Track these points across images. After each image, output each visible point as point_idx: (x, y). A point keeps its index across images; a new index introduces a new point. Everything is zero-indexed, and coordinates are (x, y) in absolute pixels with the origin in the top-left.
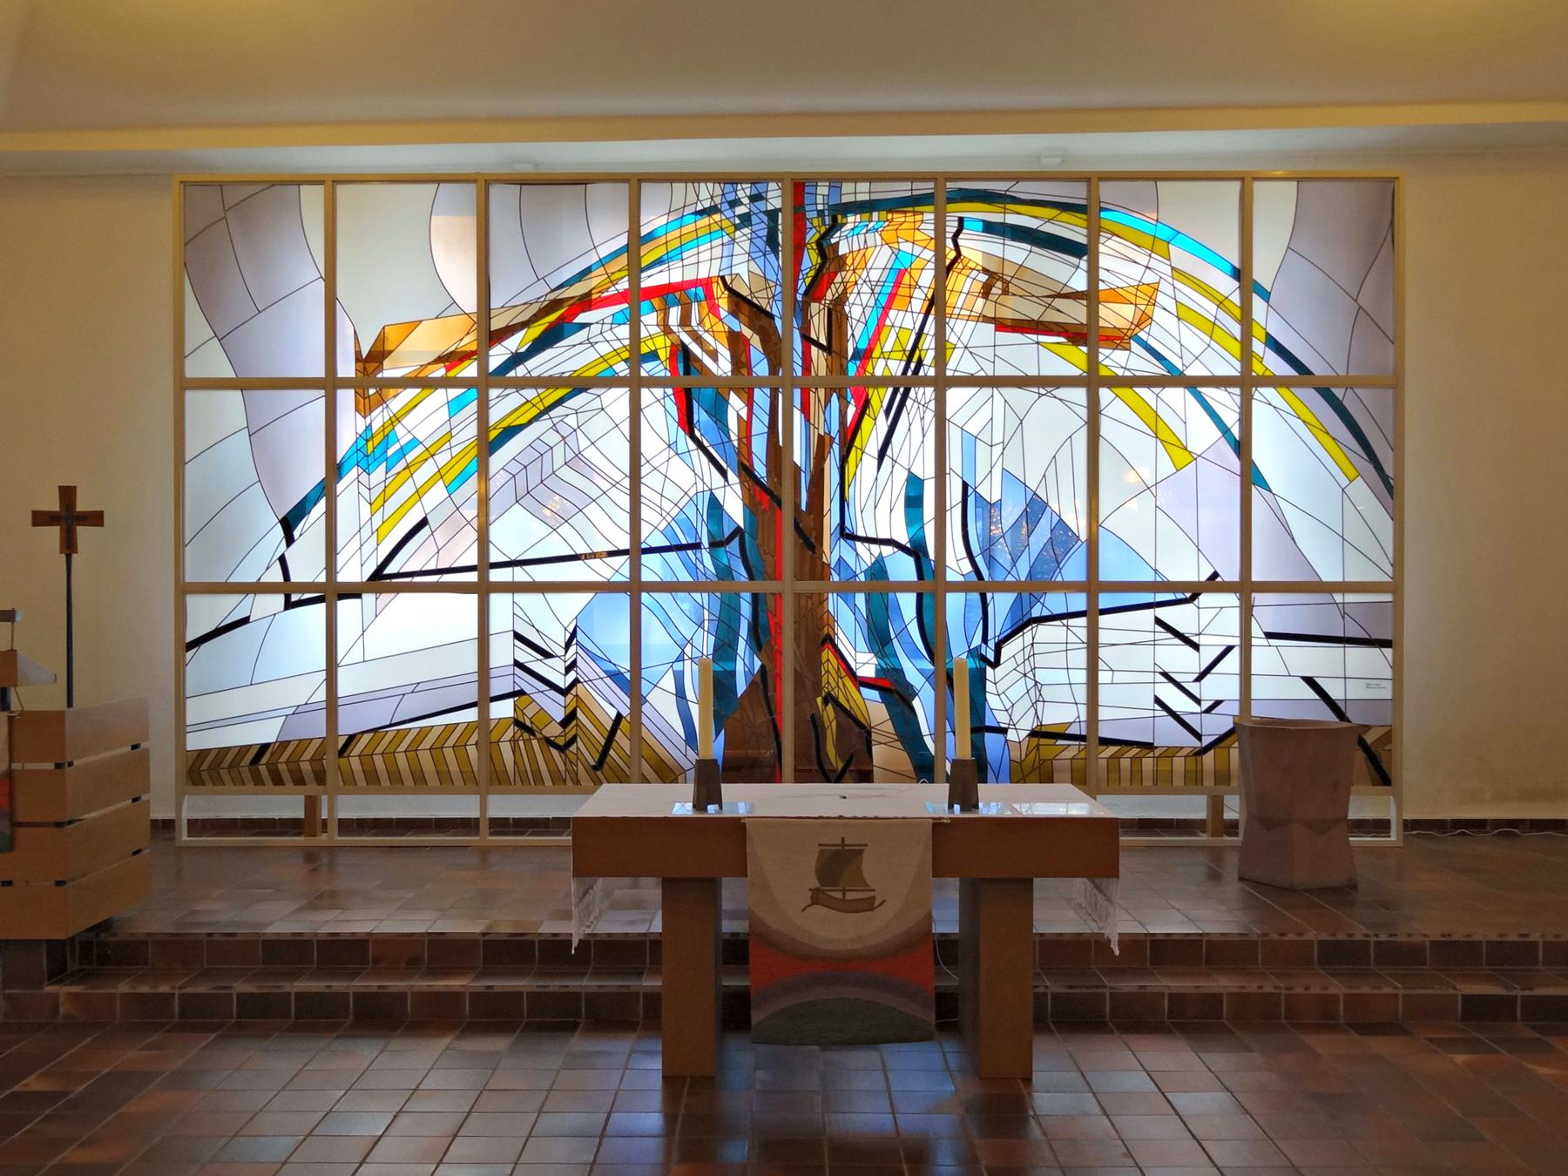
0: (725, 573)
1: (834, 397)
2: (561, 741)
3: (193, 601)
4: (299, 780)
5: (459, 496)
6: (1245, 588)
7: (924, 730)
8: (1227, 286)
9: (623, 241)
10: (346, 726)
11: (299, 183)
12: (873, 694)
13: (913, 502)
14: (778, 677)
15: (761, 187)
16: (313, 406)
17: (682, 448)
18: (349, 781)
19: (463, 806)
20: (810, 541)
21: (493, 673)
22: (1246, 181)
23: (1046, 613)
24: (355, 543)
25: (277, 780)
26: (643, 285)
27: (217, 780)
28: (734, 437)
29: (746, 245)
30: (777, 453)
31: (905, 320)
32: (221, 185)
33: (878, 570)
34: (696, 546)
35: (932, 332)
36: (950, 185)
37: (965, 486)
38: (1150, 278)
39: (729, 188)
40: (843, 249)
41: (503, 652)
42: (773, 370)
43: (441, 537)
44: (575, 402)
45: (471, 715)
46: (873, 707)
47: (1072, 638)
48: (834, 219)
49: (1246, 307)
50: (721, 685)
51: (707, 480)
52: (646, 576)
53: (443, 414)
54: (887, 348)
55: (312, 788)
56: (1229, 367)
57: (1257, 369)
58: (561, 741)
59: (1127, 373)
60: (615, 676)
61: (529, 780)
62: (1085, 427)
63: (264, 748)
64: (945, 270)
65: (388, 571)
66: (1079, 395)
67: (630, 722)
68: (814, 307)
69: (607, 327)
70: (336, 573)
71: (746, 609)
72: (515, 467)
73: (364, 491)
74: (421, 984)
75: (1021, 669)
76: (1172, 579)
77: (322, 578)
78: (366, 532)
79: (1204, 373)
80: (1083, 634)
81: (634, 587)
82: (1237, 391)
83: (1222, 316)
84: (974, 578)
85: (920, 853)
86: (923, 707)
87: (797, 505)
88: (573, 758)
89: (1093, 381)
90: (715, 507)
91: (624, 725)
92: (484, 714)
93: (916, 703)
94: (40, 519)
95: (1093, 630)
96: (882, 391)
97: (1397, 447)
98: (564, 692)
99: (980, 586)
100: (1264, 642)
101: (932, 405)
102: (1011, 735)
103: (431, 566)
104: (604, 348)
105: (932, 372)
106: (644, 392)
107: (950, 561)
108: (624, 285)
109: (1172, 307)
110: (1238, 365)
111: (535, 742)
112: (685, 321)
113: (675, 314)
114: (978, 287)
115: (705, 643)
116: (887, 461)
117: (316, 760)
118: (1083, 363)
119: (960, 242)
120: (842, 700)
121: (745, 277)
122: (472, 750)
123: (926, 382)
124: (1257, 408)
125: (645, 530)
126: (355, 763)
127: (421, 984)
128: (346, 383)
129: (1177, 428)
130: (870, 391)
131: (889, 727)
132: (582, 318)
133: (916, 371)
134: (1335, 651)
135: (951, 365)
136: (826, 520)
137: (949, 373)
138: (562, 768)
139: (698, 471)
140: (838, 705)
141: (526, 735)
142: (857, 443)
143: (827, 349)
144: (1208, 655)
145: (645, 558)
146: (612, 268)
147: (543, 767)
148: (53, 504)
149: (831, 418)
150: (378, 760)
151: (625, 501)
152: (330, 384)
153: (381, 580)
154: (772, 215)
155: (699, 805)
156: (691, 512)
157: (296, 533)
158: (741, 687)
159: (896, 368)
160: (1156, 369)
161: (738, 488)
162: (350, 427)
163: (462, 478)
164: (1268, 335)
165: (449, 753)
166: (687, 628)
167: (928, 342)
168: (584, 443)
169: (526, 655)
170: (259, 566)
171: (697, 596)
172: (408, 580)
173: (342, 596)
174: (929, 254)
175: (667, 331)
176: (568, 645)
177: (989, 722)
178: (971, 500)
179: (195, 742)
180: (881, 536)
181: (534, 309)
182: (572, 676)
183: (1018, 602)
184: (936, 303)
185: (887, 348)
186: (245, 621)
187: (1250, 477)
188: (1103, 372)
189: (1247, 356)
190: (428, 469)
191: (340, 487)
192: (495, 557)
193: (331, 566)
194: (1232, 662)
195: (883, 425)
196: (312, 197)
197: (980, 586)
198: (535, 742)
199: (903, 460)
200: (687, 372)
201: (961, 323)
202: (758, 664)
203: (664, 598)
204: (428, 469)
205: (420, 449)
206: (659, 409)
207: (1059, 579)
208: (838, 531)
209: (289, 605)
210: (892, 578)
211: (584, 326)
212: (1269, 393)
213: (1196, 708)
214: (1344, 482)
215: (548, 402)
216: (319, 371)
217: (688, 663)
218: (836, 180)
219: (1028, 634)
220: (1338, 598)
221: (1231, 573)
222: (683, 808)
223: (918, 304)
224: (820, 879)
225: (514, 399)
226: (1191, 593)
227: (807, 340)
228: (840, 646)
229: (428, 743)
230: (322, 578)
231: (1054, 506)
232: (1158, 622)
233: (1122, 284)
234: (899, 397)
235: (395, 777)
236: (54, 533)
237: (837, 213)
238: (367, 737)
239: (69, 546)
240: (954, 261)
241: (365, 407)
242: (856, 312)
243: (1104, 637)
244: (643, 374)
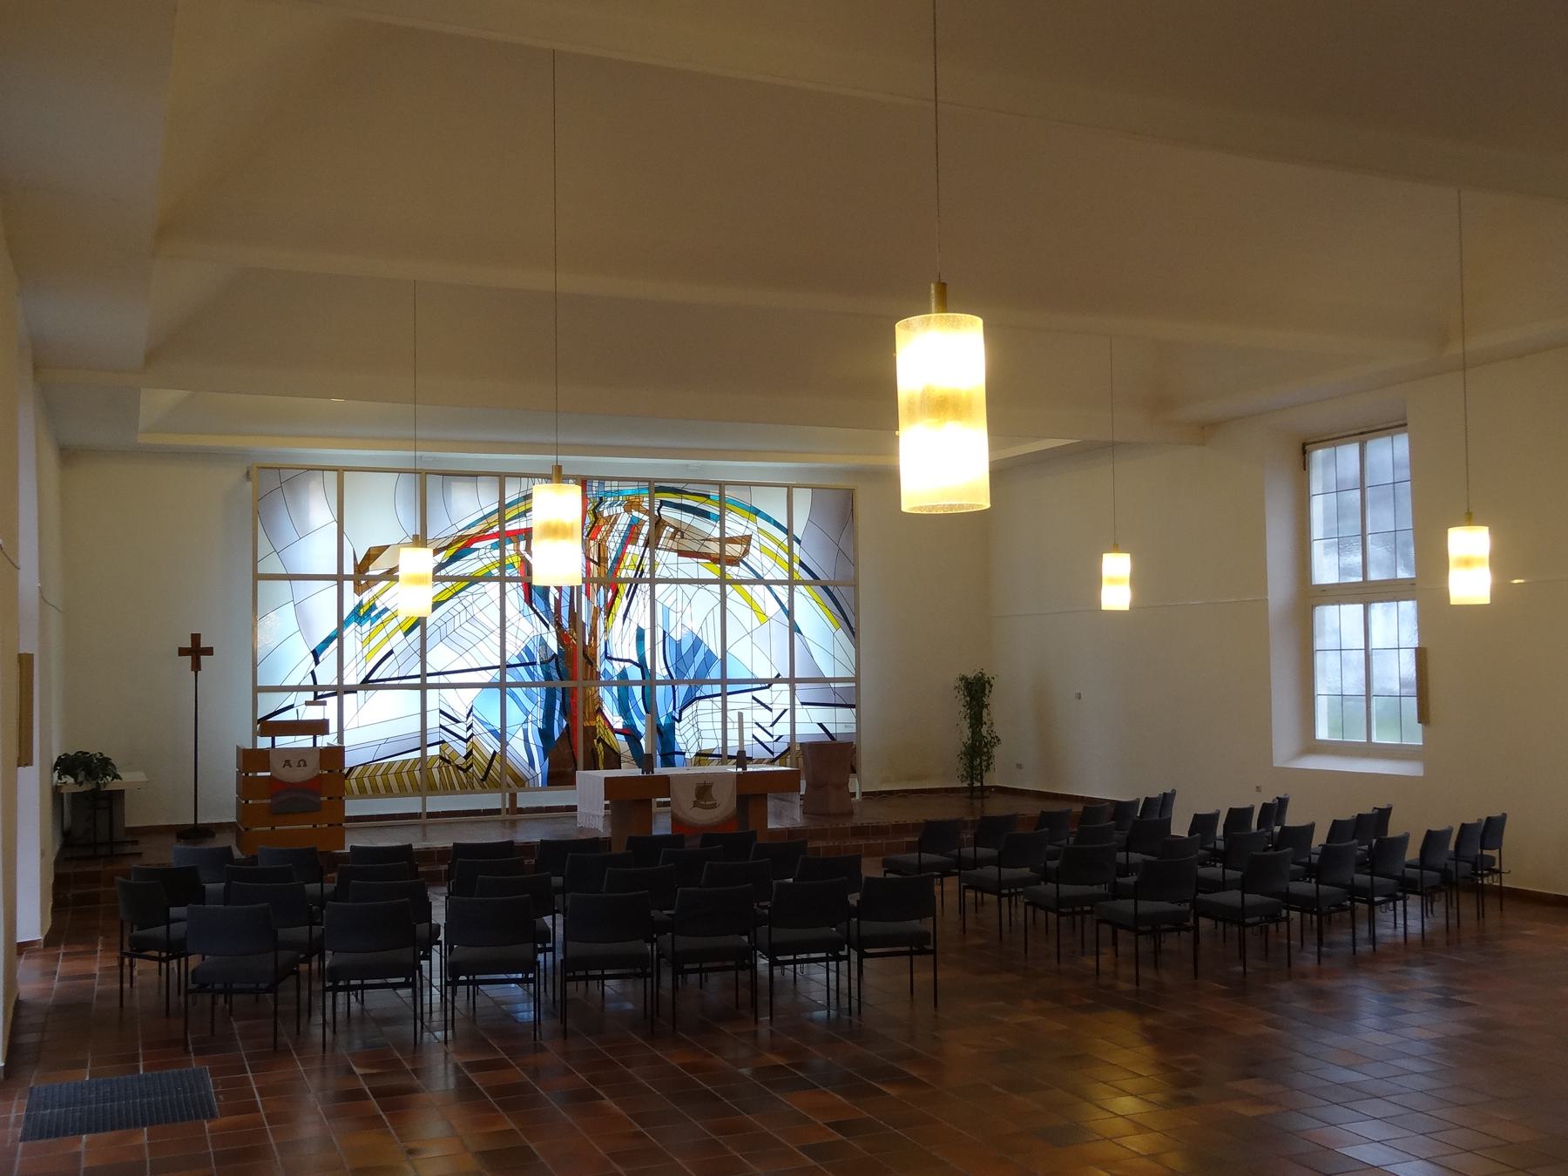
0: (548, 677)
2: (464, 767)
3: (260, 696)
6: (792, 681)
8: (782, 536)
9: (496, 506)
11: (323, 470)
12: (621, 737)
16: (331, 589)
19: (411, 805)
20: (590, 661)
22: (790, 488)
23: (703, 695)
24: (354, 664)
26: (507, 529)
28: (552, 608)
30: (574, 616)
31: (634, 551)
32: (279, 469)
33: (623, 674)
34: (534, 664)
35: (648, 556)
36: (656, 484)
37: (664, 632)
38: (748, 533)
40: (606, 514)
41: (434, 720)
44: (471, 589)
45: (417, 754)
46: (621, 742)
47: (715, 707)
49: (791, 547)
50: (545, 734)
51: (539, 630)
52: (509, 679)
54: (627, 564)
56: (784, 576)
57: (796, 577)
58: (464, 767)
59: (738, 578)
60: (493, 732)
61: (447, 789)
62: (719, 605)
65: (373, 677)
66: (716, 588)
67: (501, 756)
69: (488, 551)
70: (343, 679)
71: (559, 694)
72: (439, 623)
73: (359, 636)
75: (691, 722)
76: (759, 677)
77: (335, 683)
78: (360, 657)
79: (771, 578)
80: (720, 705)
81: (502, 686)
82: (787, 587)
83: (780, 551)
87: (584, 642)
88: (470, 775)
89: (723, 581)
90: (544, 644)
91: (497, 757)
93: (642, 741)
94: (182, 652)
95: (724, 703)
96: (624, 585)
97: (856, 614)
98: (466, 741)
99: (671, 682)
100: (801, 707)
101: (649, 593)
102: (687, 756)
103: (395, 675)
104: (487, 562)
105: (648, 576)
106: (507, 584)
107: (658, 670)
108: (496, 529)
109: (757, 545)
110: (787, 575)
111: (450, 767)
113: (523, 544)
115: (538, 713)
116: (627, 620)
118: (718, 572)
119: (661, 512)
120: (606, 740)
122: (417, 773)
123: (645, 581)
124: (796, 595)
125: (508, 655)
126: (353, 783)
128: (349, 578)
129: (761, 604)
131: (629, 753)
132: (475, 546)
133: (641, 576)
134: (831, 710)
135: (657, 573)
136: (598, 649)
137: (656, 577)
138: (465, 781)
139: (534, 625)
140: (604, 743)
141: (446, 764)
143: (598, 564)
144: (776, 714)
146: (491, 519)
147: (454, 779)
148: (188, 645)
149: (601, 597)
150: (366, 780)
151: (498, 641)
152: (339, 578)
153: (367, 683)
156: (531, 648)
157: (320, 659)
158: (557, 735)
159: (631, 574)
160: (752, 577)
161: (555, 634)
162: (351, 601)
164: (800, 561)
165: (405, 775)
166: (529, 705)
167: (646, 561)
168: (476, 610)
169: (446, 722)
170: (299, 677)
171: (534, 689)
172: (382, 683)
173: (346, 692)
175: (518, 553)
176: (467, 718)
178: (667, 639)
180: (625, 658)
182: (470, 732)
183: (690, 690)
185: (627, 564)
186: (291, 707)
187: (794, 628)
188: (728, 577)
189: (791, 570)
190: (394, 624)
191: (345, 633)
192: (429, 670)
194: (787, 716)
195: (625, 602)
198: (450, 767)
199: (635, 619)
201: (662, 552)
202: (565, 723)
203: (518, 691)
205: (389, 613)
206: (515, 593)
208: (604, 656)
210: (630, 679)
212: (801, 588)
213: (770, 739)
214: (834, 630)
216: (335, 572)
217: (530, 724)
218: (602, 480)
219: (694, 705)
220: (832, 685)
221: (785, 674)
223: (641, 542)
224: (697, 796)
226: (768, 684)
228: (605, 714)
229: (393, 770)
230: (335, 683)
231: (705, 641)
232: (754, 698)
233: (735, 535)
234: (633, 588)
235: (375, 789)
238: (360, 768)
241: (358, 590)
242: (612, 546)
243: (729, 706)
244: (507, 575)
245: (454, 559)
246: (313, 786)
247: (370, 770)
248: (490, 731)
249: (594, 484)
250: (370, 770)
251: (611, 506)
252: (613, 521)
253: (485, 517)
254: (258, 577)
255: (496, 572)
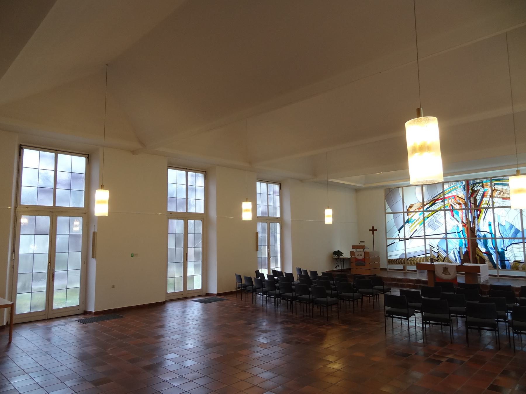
1: (475, 211)
4: (402, 264)
5: (421, 226)
7: (494, 260)
10: (408, 257)
12: (485, 255)
13: (490, 225)
14: (469, 251)
15: (462, 182)
17: (452, 219)
18: (408, 264)
21: (427, 250)
24: (408, 233)
25: (399, 263)
27: (392, 263)
29: (460, 190)
31: (486, 199)
33: (485, 236)
37: (499, 223)
39: (457, 182)
40: (475, 189)
41: (428, 247)
42: (466, 207)
43: (419, 232)
45: (424, 256)
46: (485, 256)
48: (474, 185)
52: (448, 237)
53: (418, 215)
55: (404, 265)
58: (437, 260)
60: (444, 251)
62: (520, 214)
63: (397, 259)
64: (493, 191)
65: (412, 236)
68: (471, 198)
74: (407, 284)
77: (404, 237)
80: (522, 246)
84: (501, 237)
85: (455, 269)
86: (494, 257)
91: (446, 258)
92: (426, 255)
93: (492, 256)
98: (437, 253)
101: (492, 211)
102: (510, 262)
104: (440, 206)
107: (497, 234)
108: (442, 197)
112: (452, 201)
113: (450, 201)
114: (499, 193)
117: (404, 261)
120: (480, 255)
121: (460, 194)
123: (491, 208)
126: (409, 261)
127: (407, 284)
130: (481, 210)
131: (488, 260)
132: (436, 202)
133: (489, 206)
142: (480, 217)
145: (448, 234)
148: (371, 229)
150: (412, 261)
152: (404, 212)
153: (411, 238)
154: (464, 185)
155: (431, 263)
163: (421, 224)
170: (395, 236)
173: (406, 240)
174: (490, 189)
176: (437, 246)
177: (506, 259)
178: (500, 225)
179: (389, 258)
181: (430, 201)
182: (438, 251)
184: (492, 196)
186: (394, 243)
190: (417, 223)
193: (405, 236)
195: (484, 214)
196: (400, 189)
197: (502, 238)
200: (452, 208)
204: (417, 223)
205: (415, 220)
206: (448, 213)
207: (517, 237)
209: (400, 241)
211: (437, 203)
215: (432, 214)
218: (474, 180)
219: (512, 246)
222: (430, 263)
223: (488, 196)
225: (428, 213)
227: (471, 203)
228: (479, 247)
229: (419, 259)
231: (515, 225)
236: (371, 232)
237: (474, 184)
239: (373, 234)
240: (494, 190)
241: (408, 215)
245: (431, 206)
246: (364, 260)
247: (413, 259)
248: (444, 251)
249: (471, 181)
250: (413, 259)
251: (477, 187)
252: (478, 191)
253: (439, 194)
254: (386, 213)
255: (443, 208)
